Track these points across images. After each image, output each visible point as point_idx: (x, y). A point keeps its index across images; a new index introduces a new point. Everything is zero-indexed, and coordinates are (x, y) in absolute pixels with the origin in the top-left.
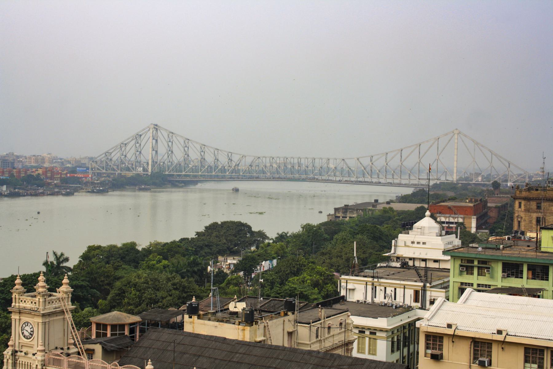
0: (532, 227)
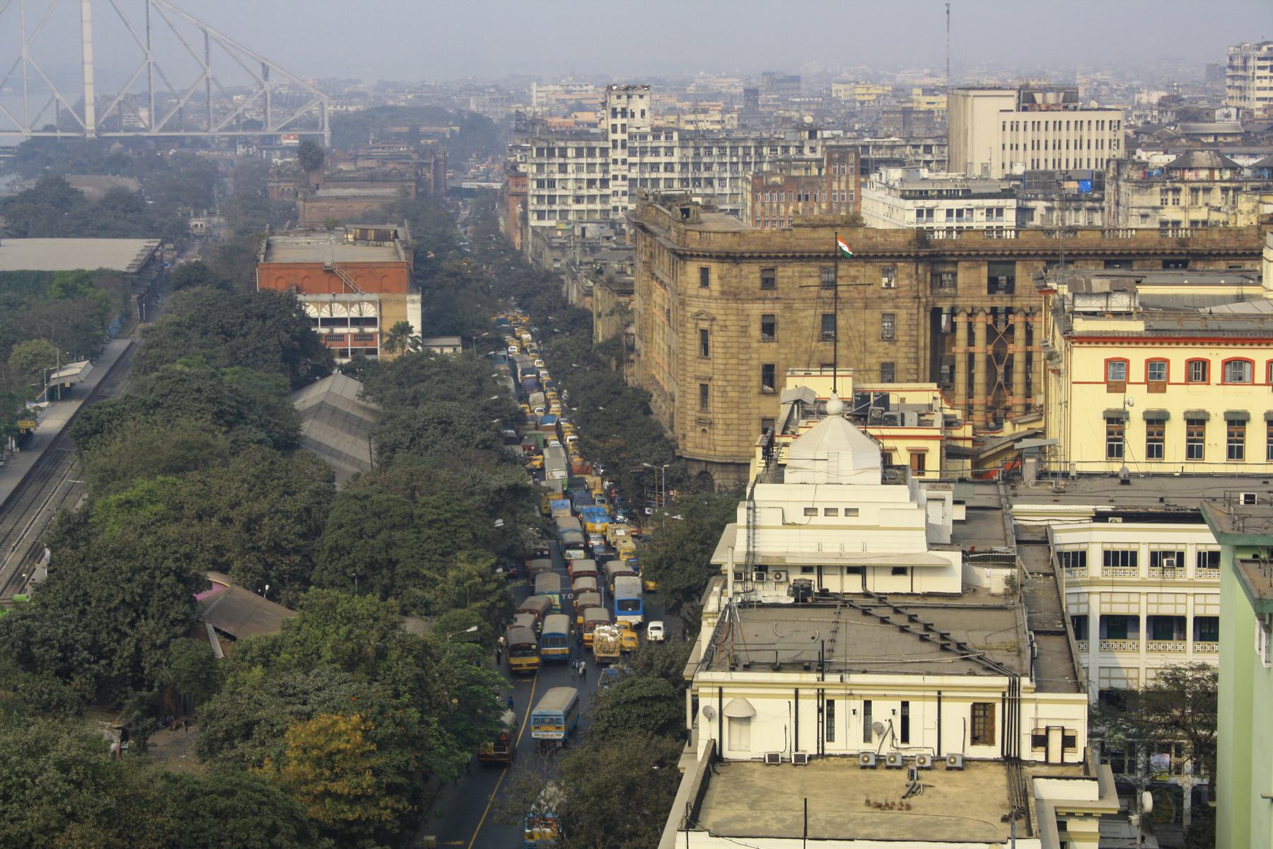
0: (749, 347)
